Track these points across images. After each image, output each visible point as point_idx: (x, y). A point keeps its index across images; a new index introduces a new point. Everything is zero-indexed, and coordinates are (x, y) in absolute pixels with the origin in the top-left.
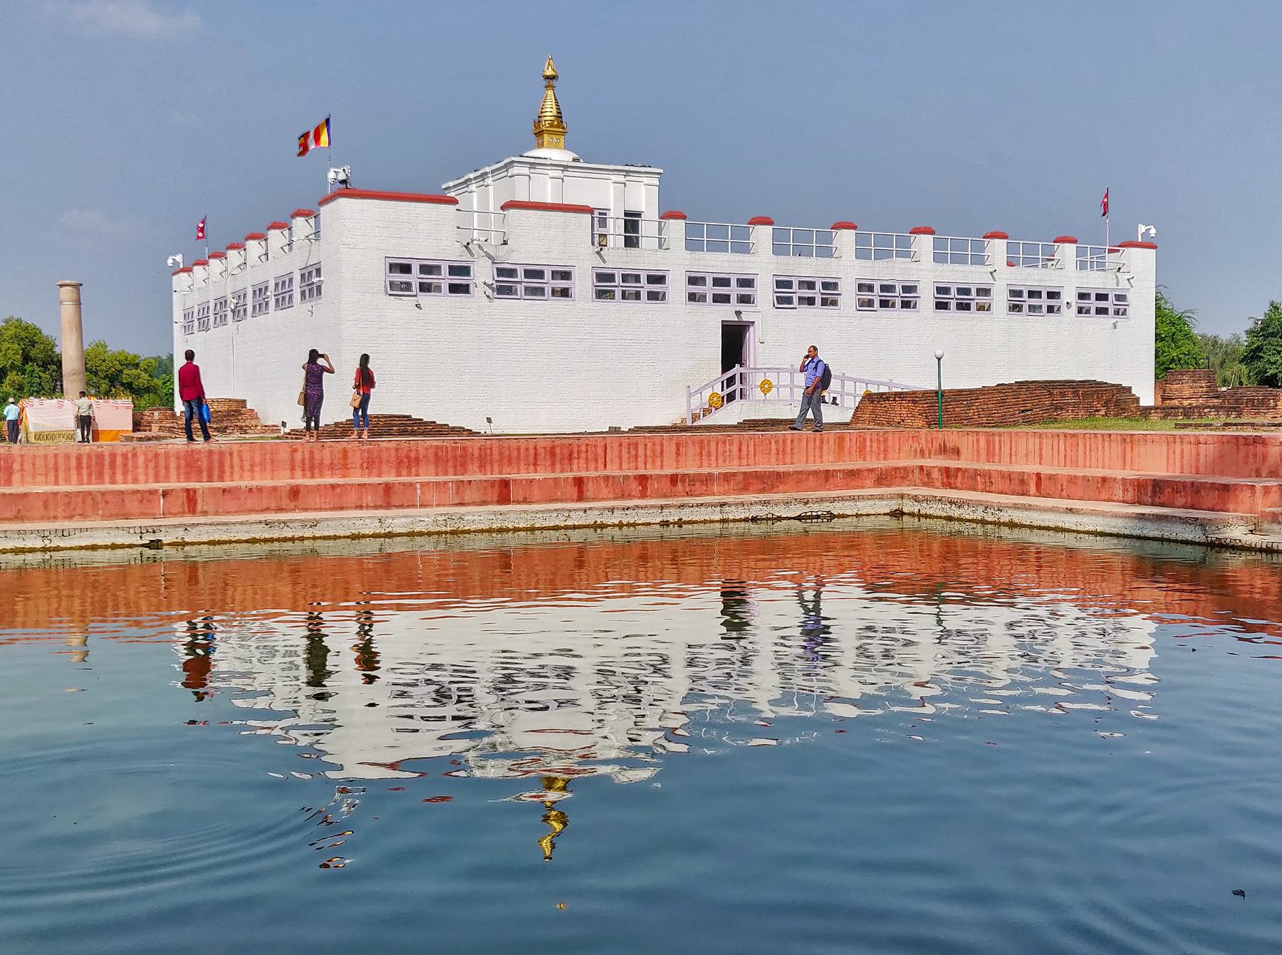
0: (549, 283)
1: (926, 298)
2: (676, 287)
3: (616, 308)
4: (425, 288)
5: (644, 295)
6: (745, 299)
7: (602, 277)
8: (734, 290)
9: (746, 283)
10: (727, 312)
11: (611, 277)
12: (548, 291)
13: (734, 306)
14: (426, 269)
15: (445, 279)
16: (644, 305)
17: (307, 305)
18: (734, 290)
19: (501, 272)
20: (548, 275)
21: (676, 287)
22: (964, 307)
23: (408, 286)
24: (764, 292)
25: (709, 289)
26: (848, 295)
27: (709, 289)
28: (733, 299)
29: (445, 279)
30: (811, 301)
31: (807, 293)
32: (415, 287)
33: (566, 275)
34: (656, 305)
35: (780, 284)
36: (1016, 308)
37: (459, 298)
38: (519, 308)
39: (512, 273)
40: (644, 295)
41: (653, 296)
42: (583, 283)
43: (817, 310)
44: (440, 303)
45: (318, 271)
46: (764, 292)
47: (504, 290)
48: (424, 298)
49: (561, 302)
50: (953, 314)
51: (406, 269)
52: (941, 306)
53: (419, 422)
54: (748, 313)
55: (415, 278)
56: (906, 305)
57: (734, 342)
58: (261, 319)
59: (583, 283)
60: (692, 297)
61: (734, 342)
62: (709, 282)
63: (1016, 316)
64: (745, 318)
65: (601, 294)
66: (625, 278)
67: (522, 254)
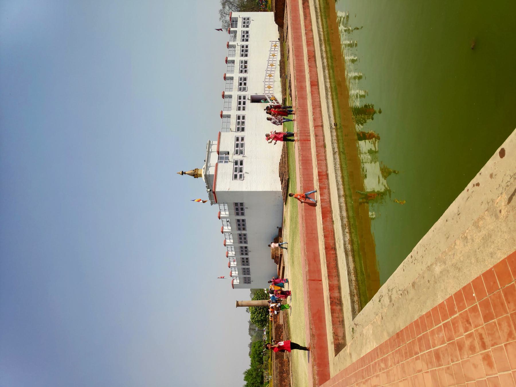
0: (240, 142)
1: (244, 59)
2: (241, 113)
3: (246, 126)
4: (241, 171)
5: (243, 121)
6: (244, 98)
7: (238, 129)
8: (242, 100)
9: (240, 98)
10: (248, 102)
11: (238, 128)
14: (236, 171)
15: (239, 166)
16: (246, 121)
17: (246, 211)
19: (237, 153)
20: (237, 142)
21: (241, 113)
22: (247, 51)
23: (241, 176)
24: (242, 93)
26: (243, 75)
27: (242, 106)
29: (239, 166)
30: (245, 84)
31: (243, 84)
32: (241, 173)
33: (237, 139)
34: (246, 118)
35: (240, 90)
36: (247, 40)
37: (244, 163)
38: (247, 149)
40: (243, 121)
43: (247, 82)
44: (246, 168)
45: (236, 204)
46: (242, 93)
47: (241, 152)
48: (244, 171)
49: (245, 139)
50: (249, 53)
51: (236, 176)
52: (246, 55)
53: (282, 160)
56: (246, 62)
57: (255, 100)
58: (249, 239)
59: (240, 134)
60: (244, 109)
63: (249, 39)
64: (250, 98)
65: (243, 129)
67: (231, 149)
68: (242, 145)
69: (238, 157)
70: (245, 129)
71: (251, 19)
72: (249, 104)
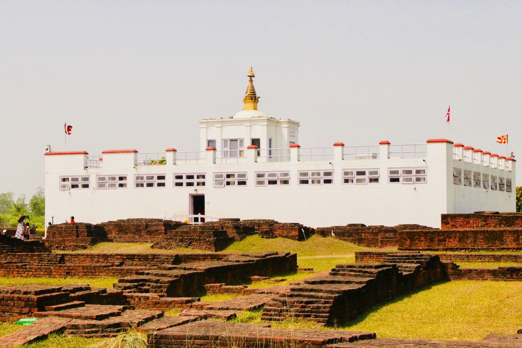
2: (170, 181)
4: (73, 186)
6: (204, 184)
8: (195, 181)
10: (191, 190)
11: (142, 178)
12: (117, 185)
13: (196, 186)
18: (195, 181)
21: (170, 181)
24: (209, 180)
25: (185, 181)
27: (185, 181)
28: (195, 184)
31: (230, 180)
39: (104, 179)
41: (159, 185)
42: (130, 182)
47: (101, 186)
54: (201, 190)
55: (69, 183)
57: (198, 204)
61: (198, 204)
62: (184, 177)
66: (148, 178)
68: (112, 186)
69: (93, 182)
70: (140, 188)
71: (418, 185)
72: (186, 192)
